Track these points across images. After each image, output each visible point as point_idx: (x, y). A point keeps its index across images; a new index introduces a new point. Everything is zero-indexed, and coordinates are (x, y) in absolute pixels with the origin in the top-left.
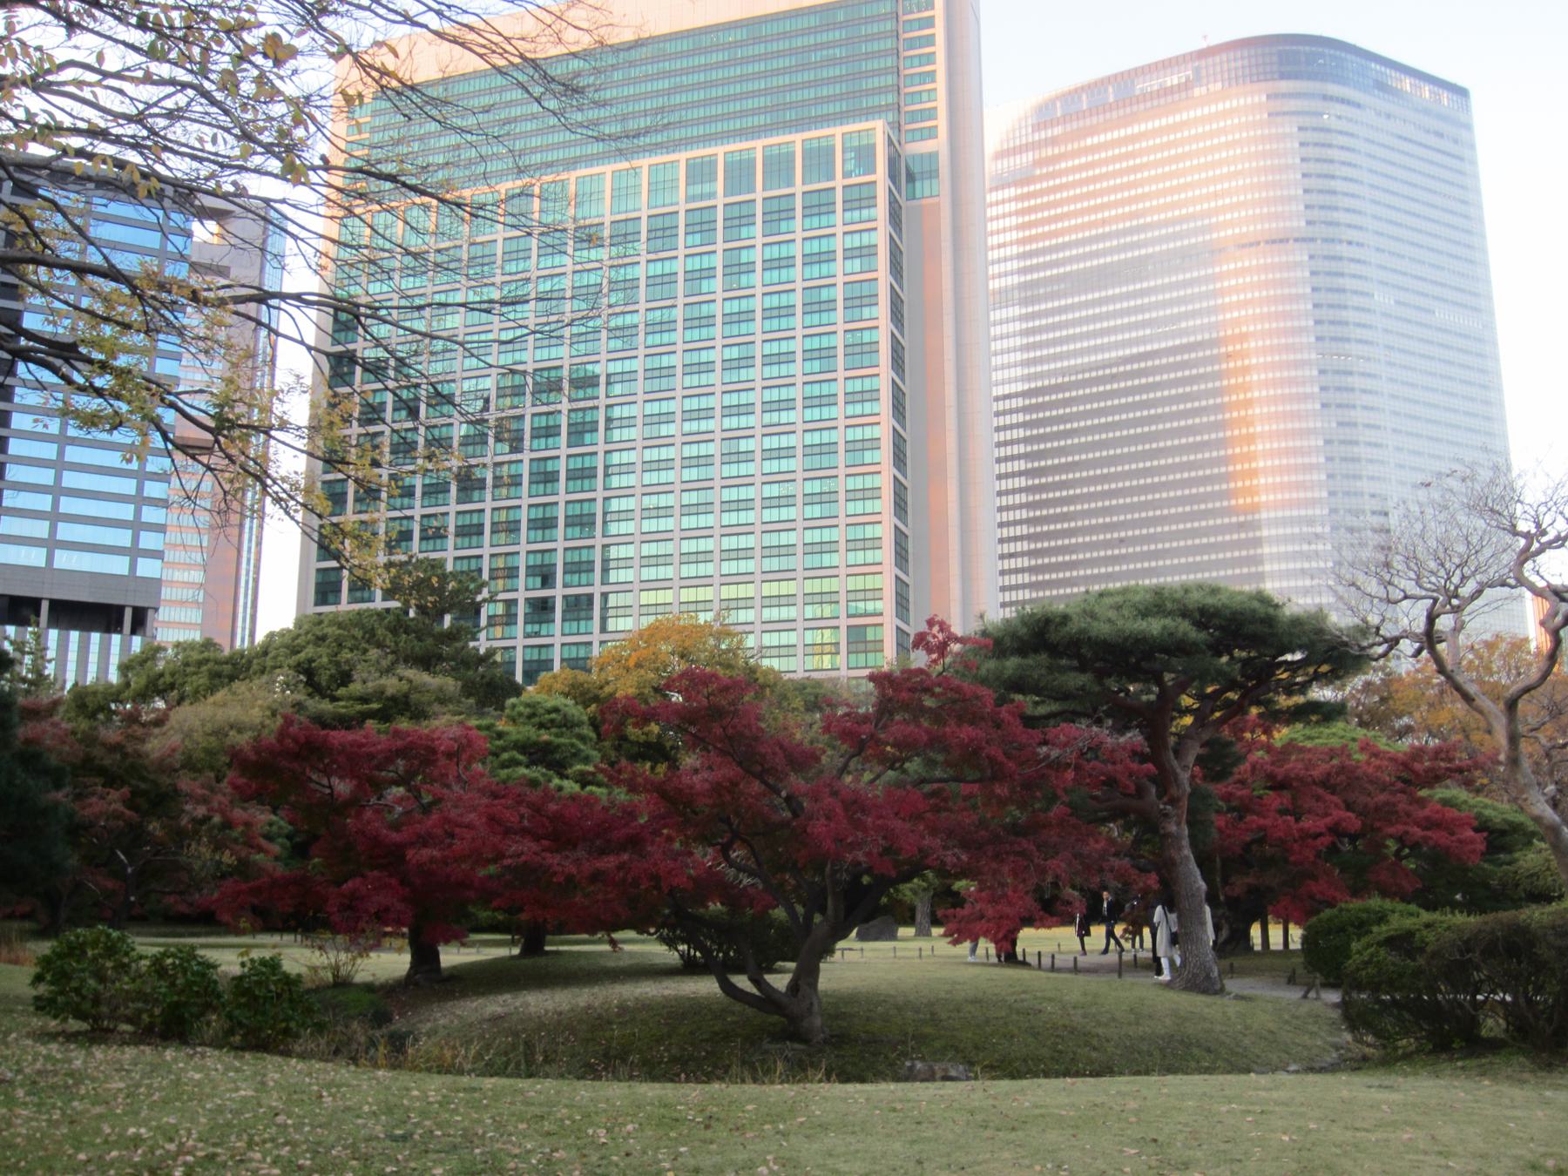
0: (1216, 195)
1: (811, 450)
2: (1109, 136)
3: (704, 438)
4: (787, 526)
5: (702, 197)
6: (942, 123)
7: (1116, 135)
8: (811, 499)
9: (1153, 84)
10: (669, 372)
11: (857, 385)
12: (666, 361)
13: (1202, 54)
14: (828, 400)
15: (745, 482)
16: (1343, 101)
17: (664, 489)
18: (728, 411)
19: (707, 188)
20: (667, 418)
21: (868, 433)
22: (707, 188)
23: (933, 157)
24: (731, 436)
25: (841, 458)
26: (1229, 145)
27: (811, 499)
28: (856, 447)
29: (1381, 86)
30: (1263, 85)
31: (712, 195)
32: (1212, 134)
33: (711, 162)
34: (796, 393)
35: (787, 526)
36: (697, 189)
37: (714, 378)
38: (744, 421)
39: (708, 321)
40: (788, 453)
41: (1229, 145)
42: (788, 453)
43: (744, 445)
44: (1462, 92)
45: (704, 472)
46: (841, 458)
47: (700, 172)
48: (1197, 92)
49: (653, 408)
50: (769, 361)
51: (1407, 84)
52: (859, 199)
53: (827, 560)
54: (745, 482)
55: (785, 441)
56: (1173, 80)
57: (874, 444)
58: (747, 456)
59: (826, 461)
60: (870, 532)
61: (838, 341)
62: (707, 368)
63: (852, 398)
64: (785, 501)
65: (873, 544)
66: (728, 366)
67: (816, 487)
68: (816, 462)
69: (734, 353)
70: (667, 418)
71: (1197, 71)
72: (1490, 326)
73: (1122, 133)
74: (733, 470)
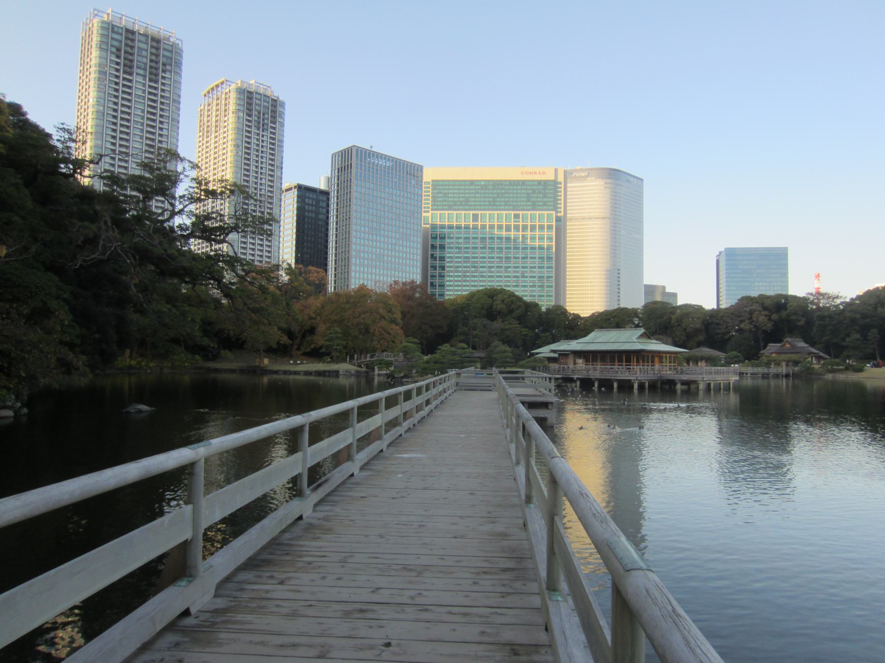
3: (518, 272)
4: (534, 291)
6: (562, 210)
9: (578, 175)
10: (510, 258)
13: (590, 169)
14: (543, 267)
15: (526, 281)
17: (509, 281)
18: (523, 267)
20: (510, 267)
24: (523, 273)
28: (548, 277)
34: (537, 265)
35: (534, 291)
39: (518, 248)
40: (534, 277)
42: (534, 277)
44: (642, 180)
47: (516, 216)
50: (531, 258)
51: (632, 179)
52: (550, 227)
54: (526, 281)
56: (583, 174)
58: (526, 277)
62: (518, 258)
63: (548, 268)
64: (534, 286)
65: (551, 296)
66: (523, 258)
70: (510, 267)
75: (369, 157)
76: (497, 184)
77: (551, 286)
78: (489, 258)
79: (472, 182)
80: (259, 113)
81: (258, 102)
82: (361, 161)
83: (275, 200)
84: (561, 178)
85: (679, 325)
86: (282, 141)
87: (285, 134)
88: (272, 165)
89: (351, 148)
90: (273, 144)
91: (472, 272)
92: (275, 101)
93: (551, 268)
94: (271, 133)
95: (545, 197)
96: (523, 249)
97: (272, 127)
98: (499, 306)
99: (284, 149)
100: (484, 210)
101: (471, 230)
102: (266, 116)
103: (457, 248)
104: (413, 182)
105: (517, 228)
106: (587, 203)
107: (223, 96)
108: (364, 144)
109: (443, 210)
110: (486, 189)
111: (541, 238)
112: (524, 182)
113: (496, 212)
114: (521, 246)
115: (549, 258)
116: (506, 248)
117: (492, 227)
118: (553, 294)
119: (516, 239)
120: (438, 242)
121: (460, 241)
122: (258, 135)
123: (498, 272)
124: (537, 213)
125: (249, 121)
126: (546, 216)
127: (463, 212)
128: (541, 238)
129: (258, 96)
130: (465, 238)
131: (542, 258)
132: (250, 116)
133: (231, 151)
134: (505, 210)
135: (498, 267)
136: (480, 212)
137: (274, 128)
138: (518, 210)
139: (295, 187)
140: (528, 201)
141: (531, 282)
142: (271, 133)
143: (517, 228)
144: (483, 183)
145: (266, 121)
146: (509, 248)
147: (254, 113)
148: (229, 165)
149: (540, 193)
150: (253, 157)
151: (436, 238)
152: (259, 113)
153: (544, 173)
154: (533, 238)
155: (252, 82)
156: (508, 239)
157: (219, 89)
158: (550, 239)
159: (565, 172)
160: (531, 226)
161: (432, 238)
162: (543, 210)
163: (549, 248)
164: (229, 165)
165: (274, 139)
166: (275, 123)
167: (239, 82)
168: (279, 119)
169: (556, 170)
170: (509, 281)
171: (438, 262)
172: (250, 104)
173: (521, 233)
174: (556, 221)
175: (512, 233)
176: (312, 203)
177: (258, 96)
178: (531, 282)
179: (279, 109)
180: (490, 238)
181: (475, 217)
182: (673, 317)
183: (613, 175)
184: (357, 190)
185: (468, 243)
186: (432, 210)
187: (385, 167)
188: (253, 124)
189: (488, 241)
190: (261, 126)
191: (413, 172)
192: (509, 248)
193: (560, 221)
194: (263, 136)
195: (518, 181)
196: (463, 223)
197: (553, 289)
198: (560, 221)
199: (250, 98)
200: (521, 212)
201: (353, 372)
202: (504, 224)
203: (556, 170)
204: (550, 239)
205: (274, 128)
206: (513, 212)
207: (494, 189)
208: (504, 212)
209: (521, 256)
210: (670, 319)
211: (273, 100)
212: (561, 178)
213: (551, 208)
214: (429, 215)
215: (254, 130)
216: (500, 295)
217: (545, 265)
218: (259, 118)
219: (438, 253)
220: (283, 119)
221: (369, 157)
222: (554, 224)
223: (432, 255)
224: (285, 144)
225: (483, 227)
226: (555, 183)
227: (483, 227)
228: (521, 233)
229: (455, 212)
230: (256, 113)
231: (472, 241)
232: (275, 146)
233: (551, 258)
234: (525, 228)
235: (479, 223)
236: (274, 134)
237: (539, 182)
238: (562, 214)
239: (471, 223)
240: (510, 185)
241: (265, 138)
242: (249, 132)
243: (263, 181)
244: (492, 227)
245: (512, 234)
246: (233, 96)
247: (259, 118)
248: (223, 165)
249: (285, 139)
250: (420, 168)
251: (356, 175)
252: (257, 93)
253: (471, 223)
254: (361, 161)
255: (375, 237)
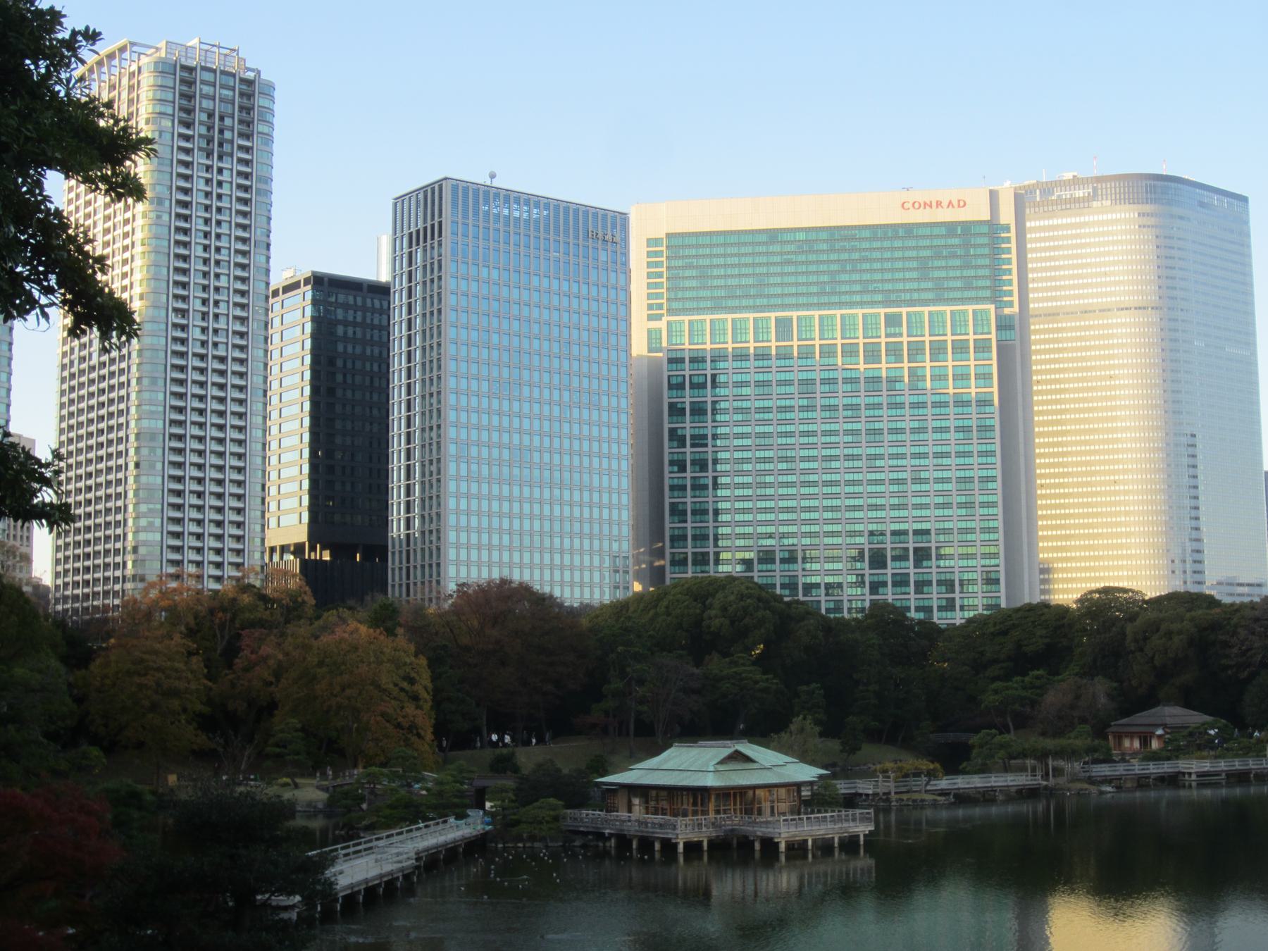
0: (1105, 274)
1: (960, 480)
2: (1037, 223)
3: (901, 469)
4: (948, 518)
5: (895, 335)
6: (1015, 298)
7: (1042, 223)
8: (960, 505)
9: (1066, 194)
10: (879, 432)
11: (984, 448)
12: (877, 426)
13: (1099, 179)
14: (968, 454)
15: (925, 494)
16: (1181, 218)
17: (881, 495)
19: (897, 330)
20: (881, 457)
21: (990, 473)
22: (897, 330)
23: (1011, 317)
24: (917, 469)
25: (976, 485)
26: (1114, 243)
27: (960, 505)
29: (1202, 204)
30: (1135, 206)
31: (901, 335)
32: (1103, 234)
33: (900, 315)
35: (948, 518)
36: (892, 330)
37: (907, 437)
38: (923, 462)
39: (900, 406)
41: (1114, 243)
43: (923, 475)
44: (1244, 199)
45: (901, 488)
46: (976, 485)
47: (893, 321)
48: (1095, 204)
49: (872, 451)
52: (982, 347)
53: (970, 537)
54: (925, 494)
55: (946, 474)
56: (1079, 193)
57: (993, 479)
58: (926, 481)
59: (968, 486)
60: (992, 524)
61: (973, 423)
62: (900, 431)
63: (982, 454)
65: (993, 530)
66: (914, 431)
67: (963, 499)
68: (962, 486)
69: (916, 425)
70: (881, 457)
71: (1095, 189)
72: (1254, 354)
73: (1046, 223)
74: (917, 487)
75: (487, 202)
76: (839, 237)
77: (992, 505)
78: (826, 433)
79: (773, 235)
80: (211, 115)
81: (207, 90)
82: (466, 217)
83: (254, 326)
84: (1007, 215)
85: (1141, 650)
86: (268, 180)
87: (276, 161)
88: (245, 241)
89: (440, 183)
90: (246, 189)
91: (782, 472)
92: (250, 83)
93: (990, 454)
94: (240, 161)
95: (967, 267)
96: (914, 405)
97: (241, 148)
98: (715, 621)
99: (274, 198)
100: (808, 306)
101: (774, 363)
102: (228, 122)
103: (738, 410)
104: (603, 256)
105: (894, 351)
106: (1090, 276)
107: (125, 81)
108: (470, 171)
109: (698, 310)
110: (811, 251)
111: (961, 377)
112: (909, 230)
113: (838, 313)
114: (908, 399)
115: (984, 429)
116: (870, 407)
117: (828, 351)
118: (998, 524)
119: (892, 381)
120: (688, 398)
121: (746, 391)
122: (208, 168)
123: (849, 470)
124: (948, 309)
125: (187, 138)
126: (973, 318)
127: (751, 316)
128: (961, 377)
129: (208, 77)
130: (759, 384)
131: (965, 429)
132: (188, 125)
133: (145, 216)
134: (861, 304)
135: (849, 457)
136: (794, 314)
137: (248, 150)
138: (898, 303)
139: (307, 281)
140: (927, 279)
141: (939, 493)
142: (240, 161)
143: (894, 351)
144: (801, 236)
145: (227, 135)
146: (878, 406)
147: (201, 117)
148: (139, 249)
149: (953, 256)
150: (198, 225)
151: (681, 386)
152: (211, 115)
153: (962, 204)
154: (939, 377)
155: (194, 42)
156: (874, 380)
157: (116, 62)
158: (984, 377)
159: (1020, 201)
160: (941, 342)
161: (671, 387)
162: (963, 301)
163: (983, 402)
164: (139, 249)
165: (246, 176)
166: (248, 137)
167: (162, 45)
168: (260, 127)
169: (993, 195)
170: (881, 495)
171: (688, 449)
172: (189, 97)
173: (906, 365)
174: (999, 328)
175: (884, 365)
176: (349, 321)
177: (208, 77)
178: (939, 493)
179: (260, 101)
180: (825, 381)
181: (784, 327)
182: (1129, 629)
183: (1159, 191)
184: (456, 286)
185: (768, 397)
186: (671, 311)
187: (528, 221)
188: (198, 143)
189: (819, 388)
190: (215, 146)
191: (600, 232)
192: (878, 406)
193: (1010, 327)
194: (220, 171)
195: (895, 227)
196: (752, 345)
197: (999, 511)
198: (1010, 327)
199: (191, 83)
200: (904, 310)
201: (320, 806)
202: (861, 341)
203: (993, 195)
204: (984, 377)
205: (248, 150)
206: (882, 311)
207: (833, 250)
208: (860, 312)
209: (907, 425)
210: (1124, 634)
211: (243, 81)
212: (1007, 215)
213: (988, 293)
214: (662, 324)
215: (199, 158)
216: (720, 595)
217: (975, 448)
218: (210, 128)
219: (688, 427)
220: (271, 124)
221: (487, 202)
222: (993, 336)
223: (672, 432)
224: (275, 186)
225: (806, 353)
226: (993, 228)
227: (806, 353)
228: (906, 365)
229: (730, 317)
230: (204, 117)
231: (776, 390)
232: (251, 192)
233: (991, 428)
234: (916, 350)
235: (795, 343)
236: (247, 163)
237: (951, 228)
238: (1016, 309)
239: (774, 344)
240: (874, 238)
241: (226, 176)
242: (187, 165)
243: (223, 282)
244: (828, 351)
245: (883, 368)
246: (147, 79)
247: (210, 128)
248: (125, 248)
249: (275, 174)
250: (620, 221)
251: (454, 253)
252: (204, 69)
253: (774, 344)
254: (466, 217)
255: (506, 404)
